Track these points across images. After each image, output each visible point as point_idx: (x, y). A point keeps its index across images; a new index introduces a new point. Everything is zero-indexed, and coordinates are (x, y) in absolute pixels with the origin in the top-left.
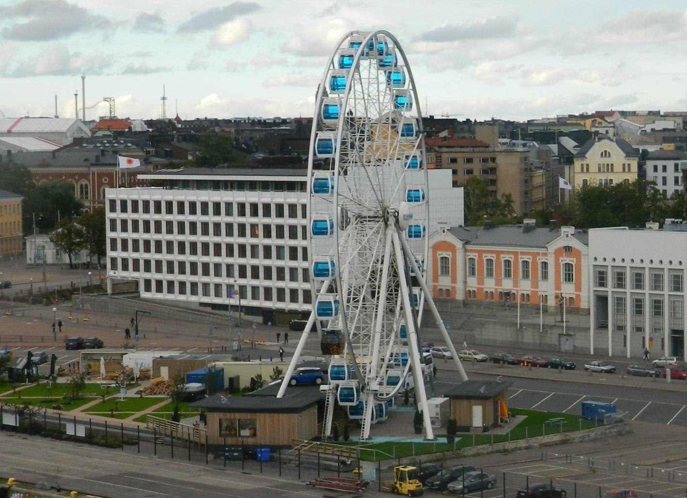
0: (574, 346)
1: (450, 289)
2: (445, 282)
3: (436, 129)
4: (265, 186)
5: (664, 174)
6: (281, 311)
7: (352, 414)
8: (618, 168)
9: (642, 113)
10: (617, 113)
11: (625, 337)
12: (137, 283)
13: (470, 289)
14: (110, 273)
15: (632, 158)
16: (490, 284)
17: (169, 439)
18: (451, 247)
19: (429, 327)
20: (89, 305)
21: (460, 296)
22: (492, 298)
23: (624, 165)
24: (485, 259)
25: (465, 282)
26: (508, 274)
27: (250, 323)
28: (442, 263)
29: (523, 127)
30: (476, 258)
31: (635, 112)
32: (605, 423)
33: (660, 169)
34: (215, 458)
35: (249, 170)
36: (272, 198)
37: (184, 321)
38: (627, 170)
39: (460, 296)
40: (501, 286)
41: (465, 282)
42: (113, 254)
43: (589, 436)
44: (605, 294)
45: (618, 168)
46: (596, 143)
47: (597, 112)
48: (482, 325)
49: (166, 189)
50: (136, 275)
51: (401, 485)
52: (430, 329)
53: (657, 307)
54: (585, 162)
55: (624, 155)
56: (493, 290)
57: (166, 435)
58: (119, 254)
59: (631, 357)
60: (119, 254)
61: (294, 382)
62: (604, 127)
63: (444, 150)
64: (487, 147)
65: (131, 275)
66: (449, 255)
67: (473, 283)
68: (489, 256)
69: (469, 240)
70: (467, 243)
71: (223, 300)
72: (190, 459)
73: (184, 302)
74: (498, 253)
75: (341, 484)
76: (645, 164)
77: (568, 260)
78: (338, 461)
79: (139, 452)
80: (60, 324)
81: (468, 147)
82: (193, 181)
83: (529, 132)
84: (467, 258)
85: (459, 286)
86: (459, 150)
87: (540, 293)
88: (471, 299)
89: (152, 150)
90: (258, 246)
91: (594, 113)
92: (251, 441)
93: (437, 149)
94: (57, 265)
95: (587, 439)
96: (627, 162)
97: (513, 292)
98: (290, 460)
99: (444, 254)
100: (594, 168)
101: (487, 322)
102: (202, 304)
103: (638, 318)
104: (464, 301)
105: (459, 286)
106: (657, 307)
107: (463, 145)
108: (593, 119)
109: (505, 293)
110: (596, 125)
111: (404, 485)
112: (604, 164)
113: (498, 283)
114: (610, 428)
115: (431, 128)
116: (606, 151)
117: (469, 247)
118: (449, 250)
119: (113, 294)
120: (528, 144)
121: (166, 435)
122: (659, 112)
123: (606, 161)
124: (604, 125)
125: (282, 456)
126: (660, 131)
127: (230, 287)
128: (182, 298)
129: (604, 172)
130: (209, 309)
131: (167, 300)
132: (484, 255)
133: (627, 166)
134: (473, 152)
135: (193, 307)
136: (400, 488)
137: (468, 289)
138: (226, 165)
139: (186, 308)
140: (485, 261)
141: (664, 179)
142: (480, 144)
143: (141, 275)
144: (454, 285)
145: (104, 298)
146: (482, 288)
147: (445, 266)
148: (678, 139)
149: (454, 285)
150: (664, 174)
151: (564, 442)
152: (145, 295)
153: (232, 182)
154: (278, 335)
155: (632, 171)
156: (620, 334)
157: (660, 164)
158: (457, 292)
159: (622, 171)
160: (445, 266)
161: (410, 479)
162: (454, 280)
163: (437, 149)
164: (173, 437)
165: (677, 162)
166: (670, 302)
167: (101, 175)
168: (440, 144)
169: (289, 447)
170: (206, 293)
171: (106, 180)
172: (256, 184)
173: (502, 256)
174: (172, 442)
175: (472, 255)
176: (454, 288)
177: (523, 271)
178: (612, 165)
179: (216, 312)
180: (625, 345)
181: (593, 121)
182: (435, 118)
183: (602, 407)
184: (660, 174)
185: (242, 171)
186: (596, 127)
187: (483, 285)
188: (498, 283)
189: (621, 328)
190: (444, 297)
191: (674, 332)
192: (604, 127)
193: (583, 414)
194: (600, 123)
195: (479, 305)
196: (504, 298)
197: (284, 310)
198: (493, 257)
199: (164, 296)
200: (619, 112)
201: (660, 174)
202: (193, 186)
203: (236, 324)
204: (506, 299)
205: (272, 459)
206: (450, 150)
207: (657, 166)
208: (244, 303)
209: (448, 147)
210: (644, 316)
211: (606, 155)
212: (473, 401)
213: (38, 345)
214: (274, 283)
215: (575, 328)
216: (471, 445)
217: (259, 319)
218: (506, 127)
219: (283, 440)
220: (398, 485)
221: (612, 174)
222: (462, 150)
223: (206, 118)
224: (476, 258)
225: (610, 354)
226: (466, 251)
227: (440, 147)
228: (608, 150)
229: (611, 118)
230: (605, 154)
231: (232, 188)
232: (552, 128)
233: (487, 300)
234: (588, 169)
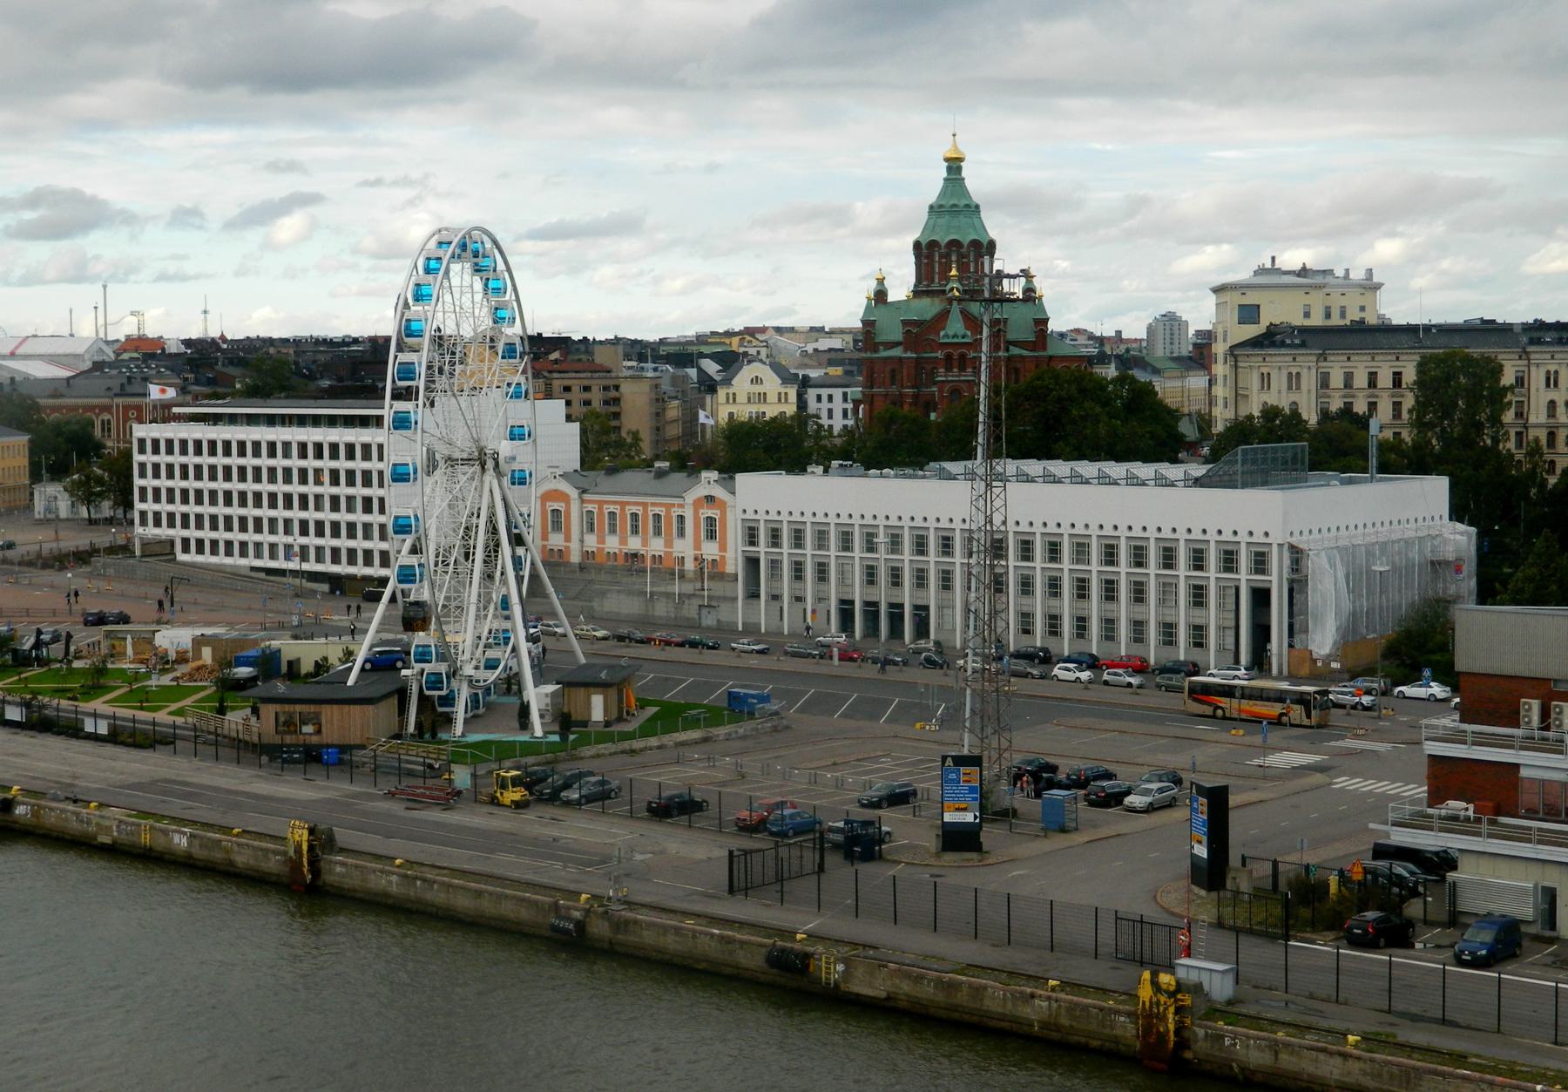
0: (718, 620)
2: (556, 540)
4: (332, 421)
5: (830, 406)
6: (352, 578)
7: (441, 705)
8: (772, 398)
9: (801, 330)
11: (781, 608)
12: (172, 543)
14: (139, 530)
16: (612, 544)
17: (212, 737)
18: (564, 497)
19: (536, 597)
20: (112, 571)
21: (575, 558)
23: (780, 394)
24: (606, 512)
25: (582, 541)
26: (635, 531)
27: (314, 592)
28: (553, 516)
29: (653, 346)
30: (595, 511)
32: (757, 716)
33: (825, 398)
34: (270, 761)
35: (313, 401)
36: (341, 437)
37: (231, 589)
39: (575, 558)
41: (582, 541)
42: (143, 506)
43: (736, 732)
44: (756, 555)
45: (772, 398)
47: (746, 328)
48: (603, 594)
50: (171, 532)
51: (502, 794)
52: (538, 600)
53: (822, 572)
54: (731, 391)
56: (617, 551)
57: (209, 733)
58: (150, 506)
59: (789, 634)
60: (150, 506)
61: (368, 666)
63: (556, 375)
64: (609, 372)
65: (164, 532)
67: (591, 542)
68: (612, 508)
70: (584, 491)
71: (280, 564)
72: (238, 763)
73: (231, 566)
74: (623, 505)
75: (428, 793)
76: (806, 392)
77: (710, 513)
78: (424, 764)
80: (76, 594)
81: (584, 372)
82: (242, 414)
83: (661, 353)
84: (585, 510)
85: (574, 546)
86: (574, 375)
87: (675, 555)
89: (191, 376)
92: (315, 740)
93: (546, 374)
94: (73, 520)
95: (733, 736)
96: (783, 390)
98: (364, 764)
99: (556, 506)
100: (741, 398)
101: (609, 590)
102: (253, 569)
103: (798, 585)
105: (574, 546)
106: (822, 572)
109: (632, 554)
111: (506, 794)
112: (754, 393)
113: (623, 541)
114: (762, 723)
116: (757, 377)
117: (586, 497)
119: (142, 556)
121: (209, 733)
122: (823, 328)
123: (758, 389)
125: (354, 758)
126: (825, 351)
127: (288, 547)
128: (228, 561)
129: (754, 403)
130: (262, 575)
131: (210, 564)
132: (605, 506)
133: (783, 395)
134: (592, 378)
135: (243, 572)
136: (500, 798)
137: (585, 549)
138: (283, 395)
139: (234, 574)
140: (606, 515)
141: (830, 411)
142: (599, 368)
143: (178, 533)
144: (568, 544)
145: (131, 561)
146: (603, 549)
147: (557, 521)
149: (568, 544)
150: (830, 406)
151: (706, 740)
152: (182, 557)
153: (291, 416)
154: (349, 607)
156: (776, 604)
157: (825, 392)
158: (572, 553)
160: (557, 521)
161: (513, 787)
162: (568, 539)
163: (546, 374)
164: (217, 735)
166: (838, 565)
167: (126, 408)
168: (550, 368)
169: (363, 747)
170: (258, 555)
171: (133, 414)
173: (627, 508)
175: (590, 507)
176: (567, 548)
177: (654, 526)
178: (765, 394)
180: (781, 619)
183: (753, 696)
184: (825, 405)
185: (304, 402)
188: (623, 541)
189: (776, 598)
190: (556, 559)
191: (843, 602)
193: (730, 705)
194: (750, 342)
195: (600, 568)
199: (207, 558)
200: (773, 328)
201: (825, 405)
204: (633, 562)
205: (341, 762)
206: (562, 375)
208: (306, 567)
209: (560, 372)
210: (805, 582)
212: (592, 689)
215: (719, 598)
216: (590, 744)
217: (325, 587)
218: (632, 347)
219: (355, 739)
220: (498, 795)
221: (765, 406)
222: (578, 375)
224: (595, 511)
225: (763, 631)
226: (583, 501)
227: (550, 372)
228: (760, 376)
230: (756, 380)
231: (291, 424)
232: (689, 348)
234: (734, 399)
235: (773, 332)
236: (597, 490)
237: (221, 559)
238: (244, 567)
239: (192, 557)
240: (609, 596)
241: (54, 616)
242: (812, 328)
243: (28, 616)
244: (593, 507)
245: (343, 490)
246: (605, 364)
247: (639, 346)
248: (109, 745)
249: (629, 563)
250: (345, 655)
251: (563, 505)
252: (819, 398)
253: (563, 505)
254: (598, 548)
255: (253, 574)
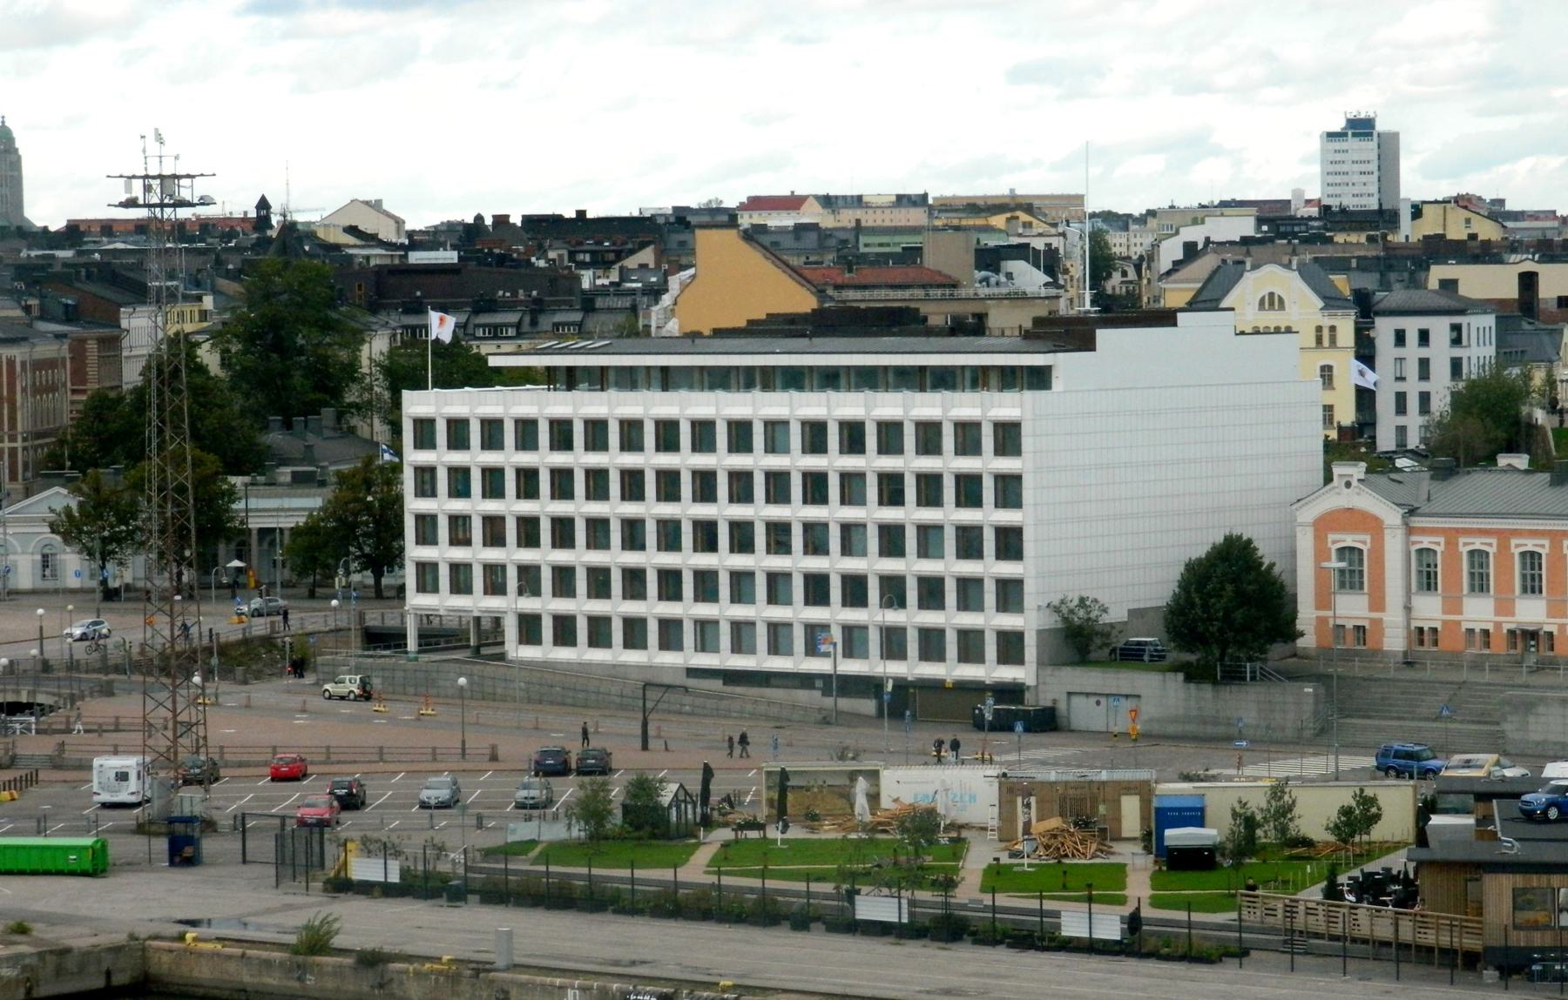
1: (1366, 624)
2: (1351, 608)
3: (614, 244)
4: (869, 379)
5: (1424, 352)
6: (934, 687)
9: (880, 201)
10: (811, 200)
13: (1420, 624)
14: (416, 600)
15: (1340, 312)
16: (1479, 612)
18: (1372, 525)
21: (1394, 641)
22: (1487, 645)
23: (1319, 329)
25: (1408, 609)
29: (842, 236)
31: (860, 198)
33: (1412, 337)
36: (945, 409)
38: (1326, 342)
39: (1394, 641)
40: (1513, 614)
41: (1408, 609)
42: (427, 553)
46: (1246, 275)
48: (1528, 707)
49: (555, 389)
55: (1321, 304)
56: (1490, 627)
58: (443, 553)
60: (443, 553)
62: (1040, 235)
64: (954, 286)
65: (478, 603)
66: (1364, 543)
67: (1429, 610)
68: (1478, 543)
69: (1416, 505)
70: (1412, 512)
74: (1504, 536)
76: (1371, 326)
79: (1292, 969)
83: (863, 250)
88: (1425, 648)
89: (33, 302)
90: (864, 526)
91: (745, 200)
93: (830, 292)
94: (46, 592)
96: (1326, 322)
97: (1547, 628)
99: (1349, 540)
101: (1542, 700)
102: (693, 672)
104: (1405, 653)
107: (898, 281)
108: (1009, 215)
110: (1020, 230)
113: (1505, 607)
115: (600, 243)
116: (1271, 295)
117: (1417, 522)
118: (1365, 531)
119: (419, 652)
120: (993, 280)
122: (925, 196)
124: (1041, 231)
128: (634, 657)
130: (716, 685)
131: (589, 665)
132: (1462, 540)
133: (1326, 334)
135: (667, 679)
137: (1415, 624)
138: (895, 330)
141: (1424, 364)
142: (940, 280)
143: (510, 604)
144: (1375, 615)
146: (1458, 623)
148: (1354, 263)
149: (1375, 615)
150: (1424, 352)
153: (1013, 370)
155: (1340, 342)
157: (1412, 325)
159: (1314, 345)
162: (1378, 603)
163: (830, 292)
165: (1457, 320)
168: (839, 281)
170: (703, 645)
172: (1018, 374)
173: (1514, 542)
174: (1345, 948)
175: (1426, 542)
176: (1377, 623)
179: (739, 690)
181: (1008, 220)
182: (589, 215)
184: (1412, 350)
185: (818, 342)
186: (1020, 235)
187: (1461, 614)
188: (1505, 607)
190: (1350, 643)
192: (1040, 235)
194: (1027, 225)
195: (1453, 661)
196: (1519, 641)
197: (943, 681)
198: (1490, 545)
199: (581, 653)
200: (817, 197)
201: (1412, 350)
202: (811, 382)
203: (824, 718)
204: (1526, 648)
207: (1404, 331)
211: (1272, 303)
213: (455, 766)
214: (912, 617)
217: (868, 706)
218: (798, 238)
223: (581, 214)
226: (1410, 531)
227: (838, 287)
228: (1278, 291)
229: (793, 213)
230: (1272, 302)
231: (749, 385)
233: (1474, 651)
235: (817, 208)
236: (1436, 507)
237: (617, 655)
238: (674, 669)
239: (547, 652)
240: (1541, 709)
241: (435, 760)
242: (900, 198)
243: (381, 760)
244: (1437, 544)
245: (910, 514)
246: (946, 271)
247: (813, 236)
248: (1122, 958)
249: (1519, 650)
250: (1358, 803)
251: (1368, 538)
252: (1400, 338)
253: (1368, 538)
254: (1445, 623)
255: (692, 683)
